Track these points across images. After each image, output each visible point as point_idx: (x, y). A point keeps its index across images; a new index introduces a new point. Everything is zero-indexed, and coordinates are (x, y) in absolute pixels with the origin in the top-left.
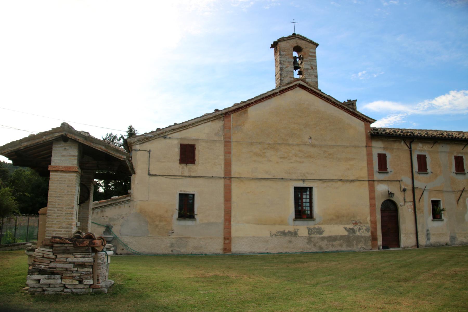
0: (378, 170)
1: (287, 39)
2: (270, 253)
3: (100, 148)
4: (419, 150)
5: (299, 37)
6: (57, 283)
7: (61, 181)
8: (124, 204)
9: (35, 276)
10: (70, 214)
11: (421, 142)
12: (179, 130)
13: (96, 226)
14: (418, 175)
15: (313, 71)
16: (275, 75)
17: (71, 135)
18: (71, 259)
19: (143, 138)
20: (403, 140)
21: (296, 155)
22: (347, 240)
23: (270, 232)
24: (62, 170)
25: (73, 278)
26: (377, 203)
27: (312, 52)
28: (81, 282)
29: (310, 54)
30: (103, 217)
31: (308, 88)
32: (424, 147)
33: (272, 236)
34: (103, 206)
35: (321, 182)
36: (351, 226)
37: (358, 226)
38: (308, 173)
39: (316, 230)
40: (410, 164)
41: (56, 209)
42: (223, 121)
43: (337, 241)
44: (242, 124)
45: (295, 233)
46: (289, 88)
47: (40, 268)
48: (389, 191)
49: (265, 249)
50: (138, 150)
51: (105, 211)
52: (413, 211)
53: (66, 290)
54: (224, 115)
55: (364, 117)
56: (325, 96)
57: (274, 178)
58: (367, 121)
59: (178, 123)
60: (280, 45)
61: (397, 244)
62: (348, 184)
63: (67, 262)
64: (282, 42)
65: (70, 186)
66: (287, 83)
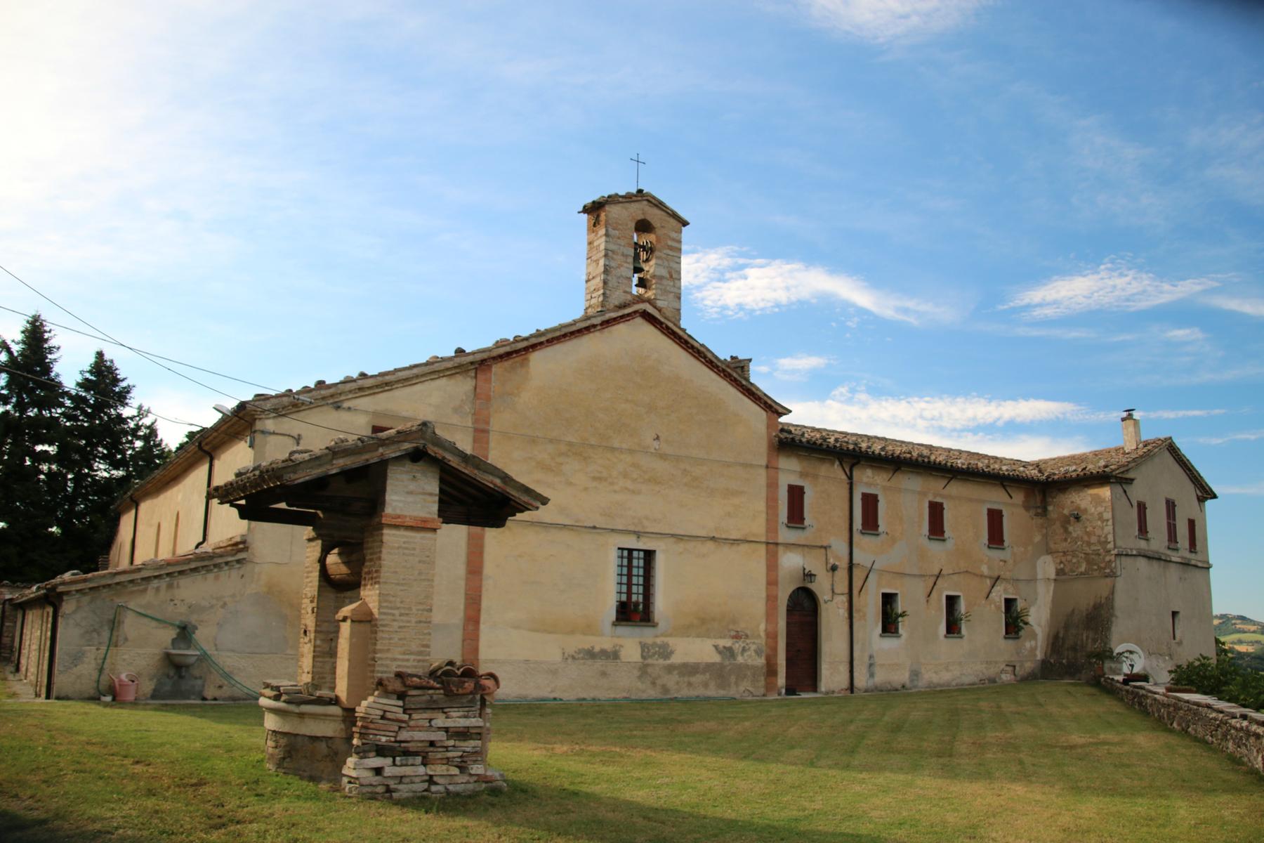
0: (786, 521)
1: (624, 200)
2: (561, 700)
3: (491, 483)
4: (866, 483)
5: (651, 199)
6: (417, 774)
7: (406, 548)
8: (230, 569)
9: (371, 759)
10: (425, 622)
11: (872, 467)
12: (372, 392)
13: (154, 624)
14: (862, 537)
15: (672, 284)
16: (584, 278)
17: (436, 449)
18: (440, 721)
19: (287, 404)
20: (838, 459)
21: (625, 475)
22: (718, 672)
23: (563, 649)
24: (411, 524)
25: (448, 761)
26: (780, 595)
27: (674, 240)
28: (463, 769)
29: (670, 243)
30: (172, 600)
31: (661, 323)
32: (876, 478)
33: (567, 659)
34: (174, 572)
35: (672, 540)
36: (727, 643)
37: (740, 643)
38: (647, 518)
39: (657, 649)
40: (847, 513)
41: (396, 612)
42: (474, 380)
43: (698, 676)
44: (516, 391)
45: (614, 655)
46: (622, 317)
47: (377, 743)
48: (804, 569)
49: (549, 689)
50: (270, 433)
51: (178, 587)
52: (846, 615)
53: (434, 788)
54: (477, 366)
55: (769, 402)
56: (696, 345)
57: (577, 524)
58: (773, 412)
59: (370, 373)
60: (609, 212)
61: (813, 685)
62: (726, 549)
63: (433, 729)
64: (612, 206)
65: (424, 562)
66: (617, 303)
